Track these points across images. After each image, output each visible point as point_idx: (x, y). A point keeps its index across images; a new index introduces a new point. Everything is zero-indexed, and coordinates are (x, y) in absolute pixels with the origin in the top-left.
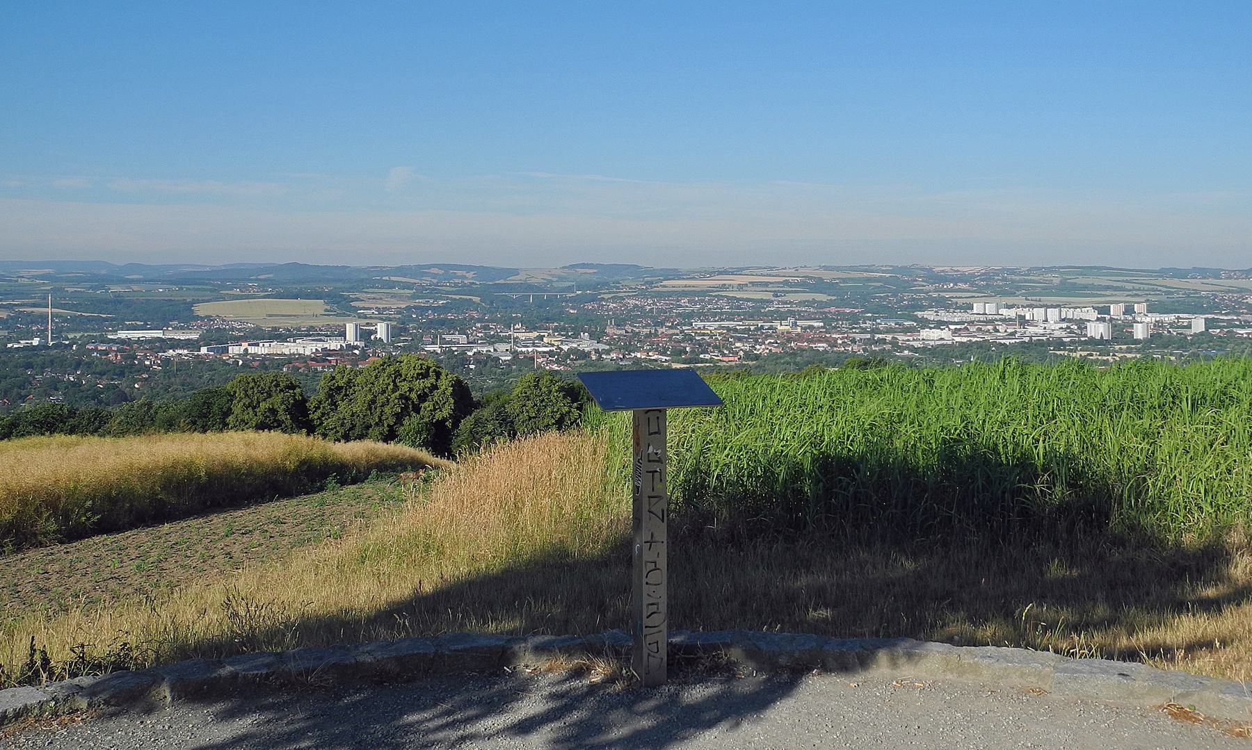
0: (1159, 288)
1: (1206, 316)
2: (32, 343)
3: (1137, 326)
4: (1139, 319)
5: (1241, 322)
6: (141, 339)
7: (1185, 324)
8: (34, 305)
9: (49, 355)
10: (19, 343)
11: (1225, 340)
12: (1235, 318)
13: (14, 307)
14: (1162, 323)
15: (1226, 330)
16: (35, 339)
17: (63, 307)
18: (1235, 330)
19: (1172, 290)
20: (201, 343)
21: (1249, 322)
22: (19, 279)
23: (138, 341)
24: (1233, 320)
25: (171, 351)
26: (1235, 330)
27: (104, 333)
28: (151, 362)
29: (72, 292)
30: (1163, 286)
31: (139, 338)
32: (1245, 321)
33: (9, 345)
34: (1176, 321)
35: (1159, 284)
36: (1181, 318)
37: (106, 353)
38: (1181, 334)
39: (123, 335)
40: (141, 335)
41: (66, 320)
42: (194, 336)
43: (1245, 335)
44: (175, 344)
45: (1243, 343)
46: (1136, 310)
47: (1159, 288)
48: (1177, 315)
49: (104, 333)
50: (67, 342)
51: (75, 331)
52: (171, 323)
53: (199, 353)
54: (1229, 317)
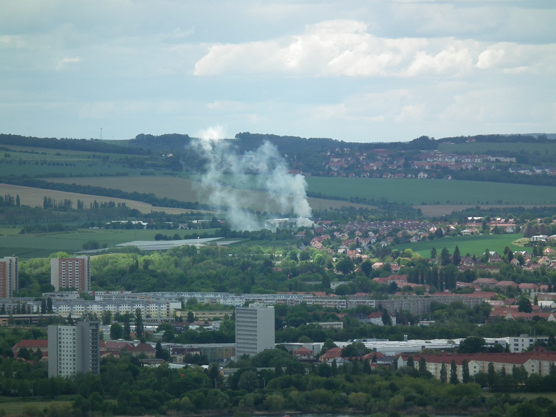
0: (132, 204)
1: (280, 297)
3: (58, 332)
4: (63, 311)
5: (386, 320)
7: (215, 326)
11: (340, 379)
12: (373, 304)
14: (139, 322)
15: (340, 344)
18: (370, 344)
19: (170, 211)
21: (414, 320)
24: (365, 312)
26: (370, 344)
30: (136, 197)
32: (403, 317)
34: (185, 314)
35: (130, 190)
36: (202, 308)
38: (200, 360)
43: (401, 363)
45: (394, 389)
46: (54, 282)
47: (132, 204)
48: (186, 296)
54: (354, 301)
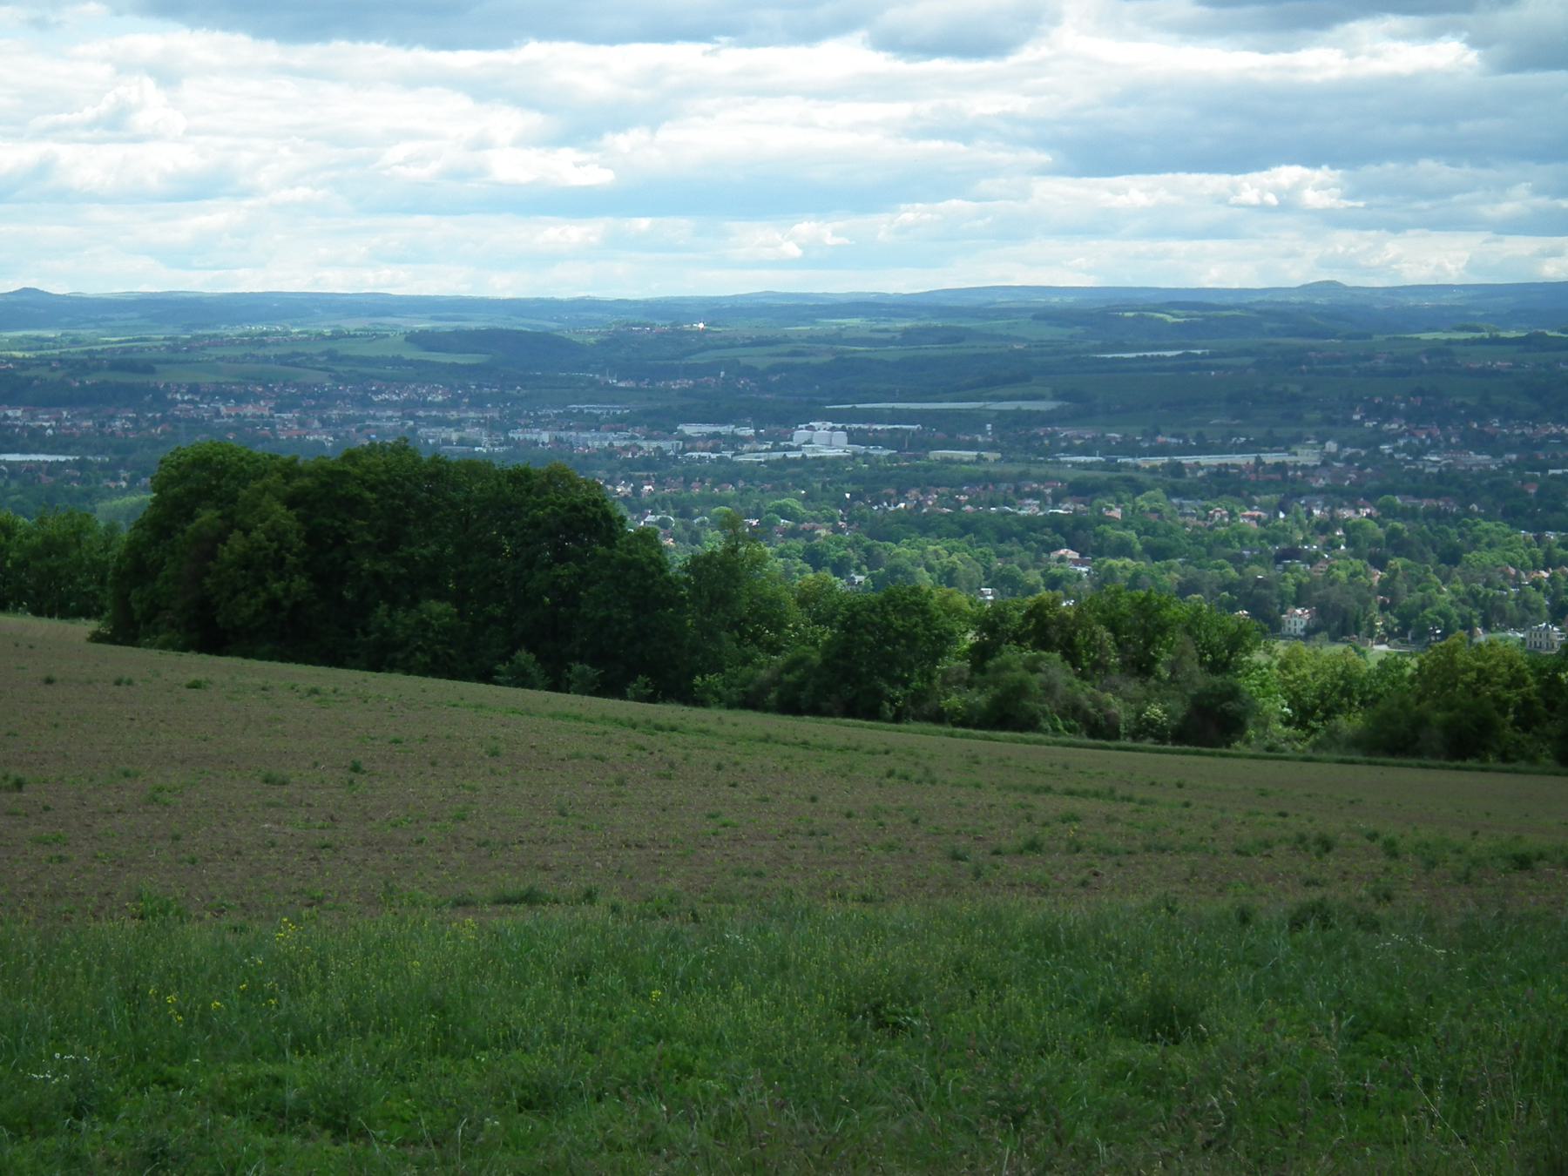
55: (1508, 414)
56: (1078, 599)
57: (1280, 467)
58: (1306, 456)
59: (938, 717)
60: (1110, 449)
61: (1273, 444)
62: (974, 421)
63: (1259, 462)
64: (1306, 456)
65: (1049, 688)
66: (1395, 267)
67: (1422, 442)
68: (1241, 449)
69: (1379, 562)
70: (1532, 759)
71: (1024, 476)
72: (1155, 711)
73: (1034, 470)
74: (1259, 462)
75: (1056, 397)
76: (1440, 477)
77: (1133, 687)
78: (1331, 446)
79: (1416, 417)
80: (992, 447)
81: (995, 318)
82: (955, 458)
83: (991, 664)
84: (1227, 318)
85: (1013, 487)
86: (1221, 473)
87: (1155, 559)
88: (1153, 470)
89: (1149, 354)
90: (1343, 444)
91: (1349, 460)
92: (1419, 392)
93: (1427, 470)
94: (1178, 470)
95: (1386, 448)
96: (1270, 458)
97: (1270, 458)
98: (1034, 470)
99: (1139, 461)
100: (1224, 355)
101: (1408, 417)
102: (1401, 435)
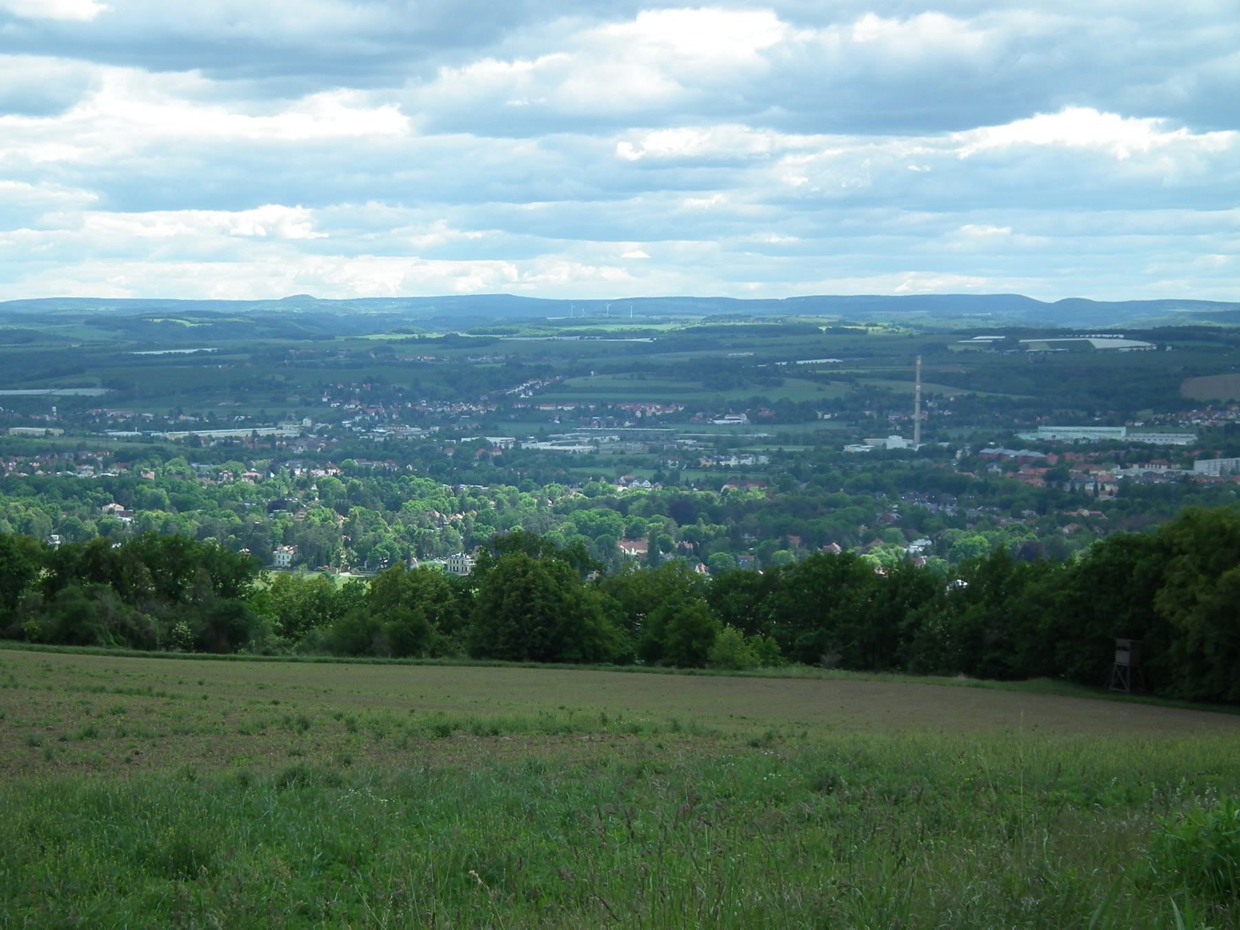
2: (885, 445)
6: (1081, 442)
8: (892, 377)
9: (913, 468)
10: (866, 444)
13: (859, 380)
16: (890, 437)
17: (943, 379)
20: (1197, 453)
22: (870, 329)
23: (1076, 447)
25: (1136, 466)
27: (1013, 431)
28: (1096, 486)
29: (960, 352)
31: (1076, 441)
33: (849, 448)
37: (1014, 466)
39: (1047, 433)
40: (1080, 435)
41: (946, 406)
42: (1181, 441)
44: (1146, 454)
49: (1013, 431)
50: (946, 444)
51: (959, 424)
52: (1139, 413)
53: (1190, 472)
55: (432, 396)
56: (123, 542)
57: (270, 438)
58: (289, 430)
59: (20, 636)
60: (145, 426)
61: (266, 421)
62: (42, 404)
63: (255, 435)
64: (289, 430)
65: (103, 611)
66: (350, 284)
67: (372, 418)
68: (242, 425)
69: (343, 510)
70: (452, 655)
71: (82, 447)
72: (182, 627)
73: (89, 443)
74: (255, 435)
75: (104, 386)
76: (386, 445)
77: (165, 608)
78: (307, 422)
79: (367, 400)
80: (57, 425)
81: (57, 323)
82: (30, 433)
83: (59, 594)
84: (229, 323)
85: (73, 456)
86: (227, 443)
87: (180, 510)
88: (177, 442)
89: (173, 351)
90: (315, 421)
91: (320, 433)
92: (370, 380)
93: (376, 440)
94: (195, 441)
95: (346, 423)
96: (263, 432)
97: (263, 432)
98: (89, 443)
99: (167, 435)
100: (228, 352)
101: (362, 400)
102: (357, 414)
